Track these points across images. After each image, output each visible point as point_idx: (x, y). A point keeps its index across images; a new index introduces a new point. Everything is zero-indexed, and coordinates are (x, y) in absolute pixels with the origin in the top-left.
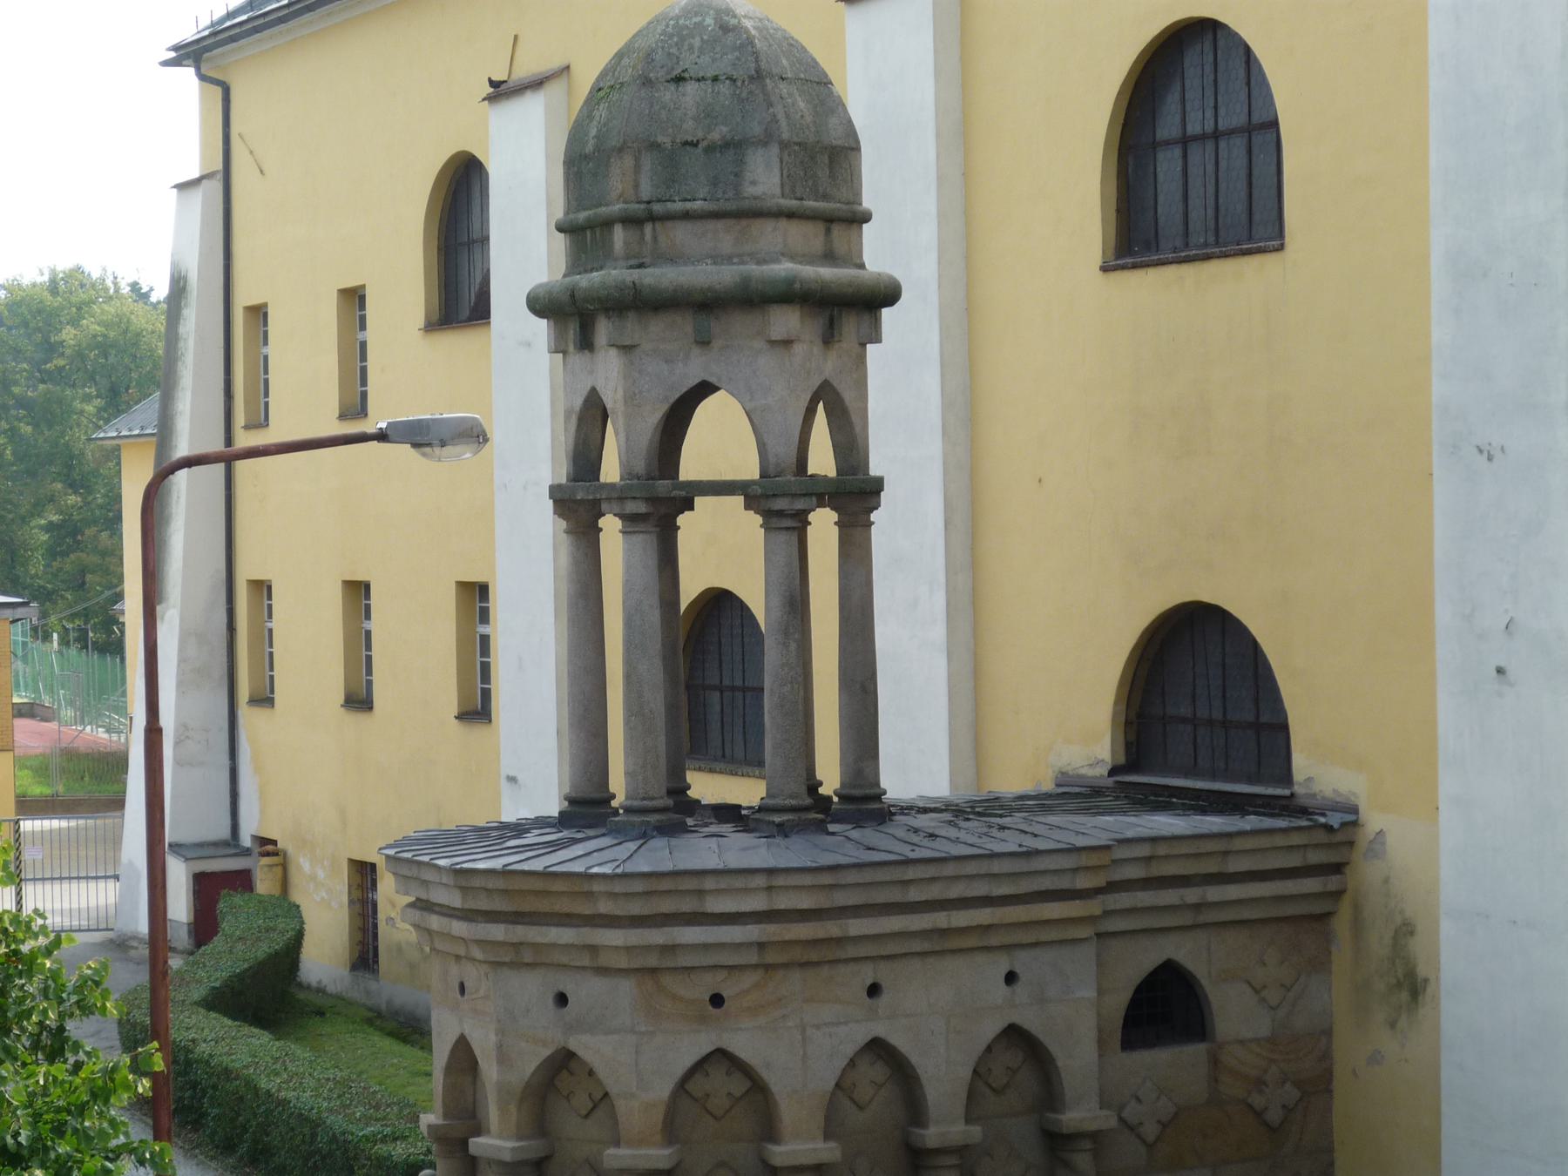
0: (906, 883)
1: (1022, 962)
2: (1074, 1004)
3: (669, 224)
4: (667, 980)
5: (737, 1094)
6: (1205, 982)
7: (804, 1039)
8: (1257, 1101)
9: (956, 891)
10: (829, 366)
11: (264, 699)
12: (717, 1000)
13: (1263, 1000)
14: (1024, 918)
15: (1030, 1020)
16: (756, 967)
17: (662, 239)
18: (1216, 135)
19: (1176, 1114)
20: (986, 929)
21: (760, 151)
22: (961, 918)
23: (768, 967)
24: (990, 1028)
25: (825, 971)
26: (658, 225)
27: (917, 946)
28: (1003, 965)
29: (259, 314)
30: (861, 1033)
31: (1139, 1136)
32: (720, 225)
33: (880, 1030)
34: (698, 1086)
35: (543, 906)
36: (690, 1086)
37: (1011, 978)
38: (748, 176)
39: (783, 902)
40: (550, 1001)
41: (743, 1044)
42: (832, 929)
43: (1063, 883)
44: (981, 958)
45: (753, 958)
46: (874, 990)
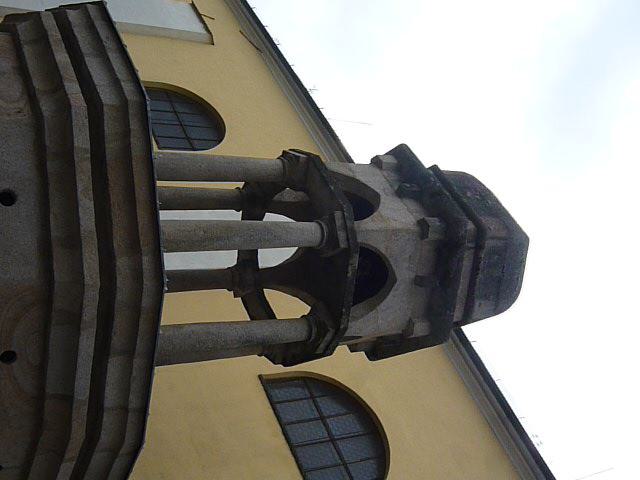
12: (9, 357)
16: (41, 388)
23: (40, 397)
35: (116, 196)
45: (51, 388)
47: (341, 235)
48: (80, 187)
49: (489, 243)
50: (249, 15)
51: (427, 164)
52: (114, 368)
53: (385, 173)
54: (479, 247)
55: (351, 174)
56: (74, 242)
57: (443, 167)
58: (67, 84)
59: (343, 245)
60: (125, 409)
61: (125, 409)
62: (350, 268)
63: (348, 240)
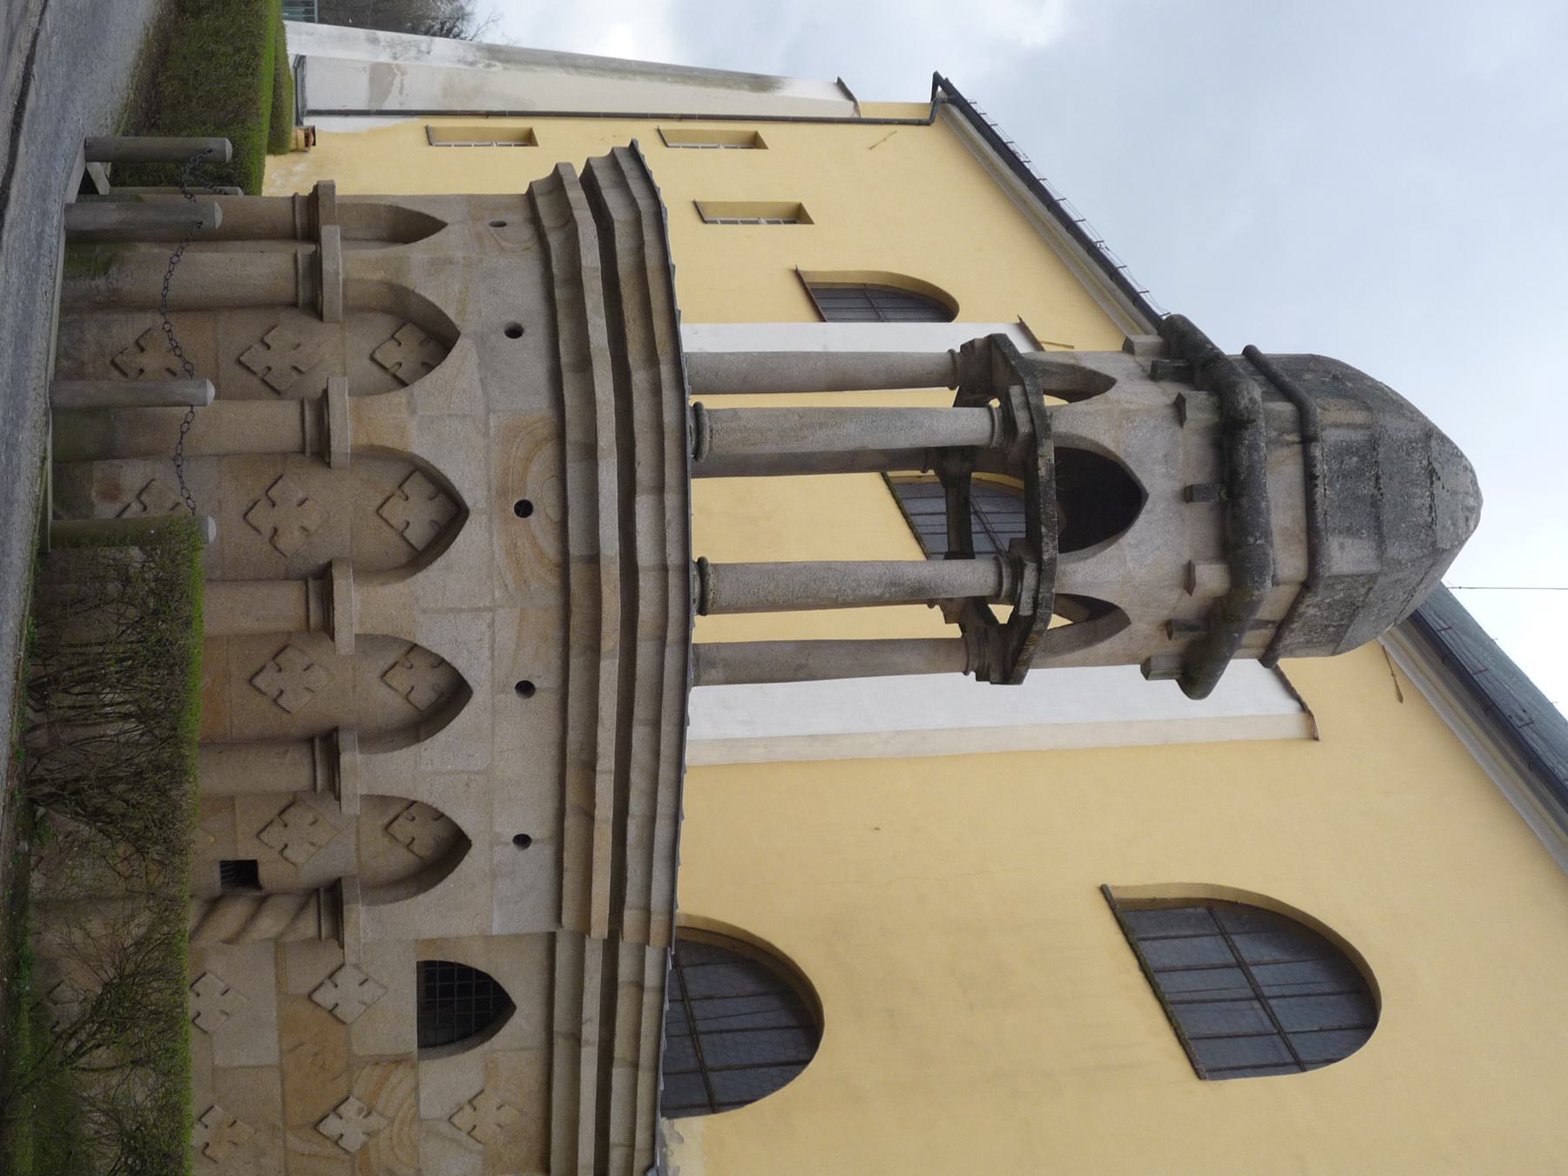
0: (656, 724)
1: (540, 854)
2: (488, 914)
3: (1299, 459)
4: (548, 452)
5: (408, 534)
6: (487, 1045)
7: (478, 609)
8: (349, 1109)
10: (1143, 628)
11: (430, 137)
12: (524, 509)
13: (461, 1109)
14: (596, 854)
15: (471, 864)
17: (1286, 451)
18: (1259, 997)
19: (344, 1023)
20: (589, 815)
21: (1372, 553)
23: (564, 567)
24: (467, 821)
25: (555, 632)
26: (1297, 448)
27: (574, 738)
28: (539, 830)
29: (755, 142)
30: (475, 675)
31: (322, 984)
32: (1300, 512)
34: (418, 488)
36: (417, 477)
37: (523, 841)
38: (1348, 541)
39: (647, 585)
40: (512, 318)
41: (471, 537)
42: (611, 640)
43: (632, 896)
44: (549, 807)
45: (574, 551)
46: (525, 688)
47: (1021, 417)
48: (589, 305)
49: (1331, 436)
50: (1134, 310)
51: (1230, 345)
52: (644, 507)
53: (1140, 359)
54: (1307, 439)
55: (1072, 362)
56: (584, 364)
57: (1266, 348)
58: (576, 213)
59: (1023, 427)
60: (664, 568)
61: (664, 568)
62: (1041, 462)
63: (1032, 421)
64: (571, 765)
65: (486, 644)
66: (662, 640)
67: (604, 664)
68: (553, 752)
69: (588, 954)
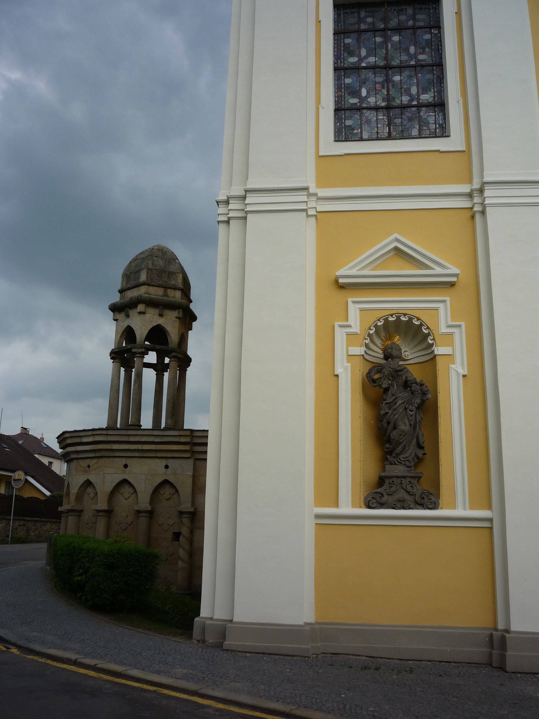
1: (170, 462)
9: (144, 439)
12: (89, 466)
14: (165, 449)
15: (171, 479)
20: (156, 451)
22: (146, 447)
24: (159, 480)
25: (112, 459)
28: (164, 462)
30: (120, 477)
33: (126, 477)
37: (167, 467)
41: (92, 479)
44: (157, 460)
46: (126, 466)
52: (85, 440)
64: (144, 455)
65: (113, 475)
66: (107, 435)
67: (114, 448)
68: (143, 459)
69: (202, 450)
